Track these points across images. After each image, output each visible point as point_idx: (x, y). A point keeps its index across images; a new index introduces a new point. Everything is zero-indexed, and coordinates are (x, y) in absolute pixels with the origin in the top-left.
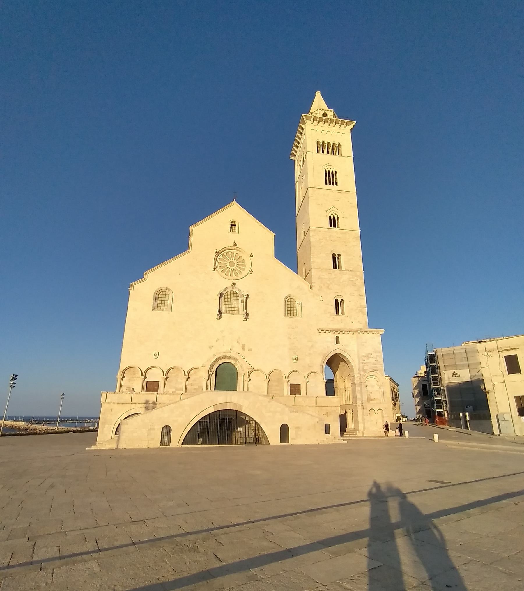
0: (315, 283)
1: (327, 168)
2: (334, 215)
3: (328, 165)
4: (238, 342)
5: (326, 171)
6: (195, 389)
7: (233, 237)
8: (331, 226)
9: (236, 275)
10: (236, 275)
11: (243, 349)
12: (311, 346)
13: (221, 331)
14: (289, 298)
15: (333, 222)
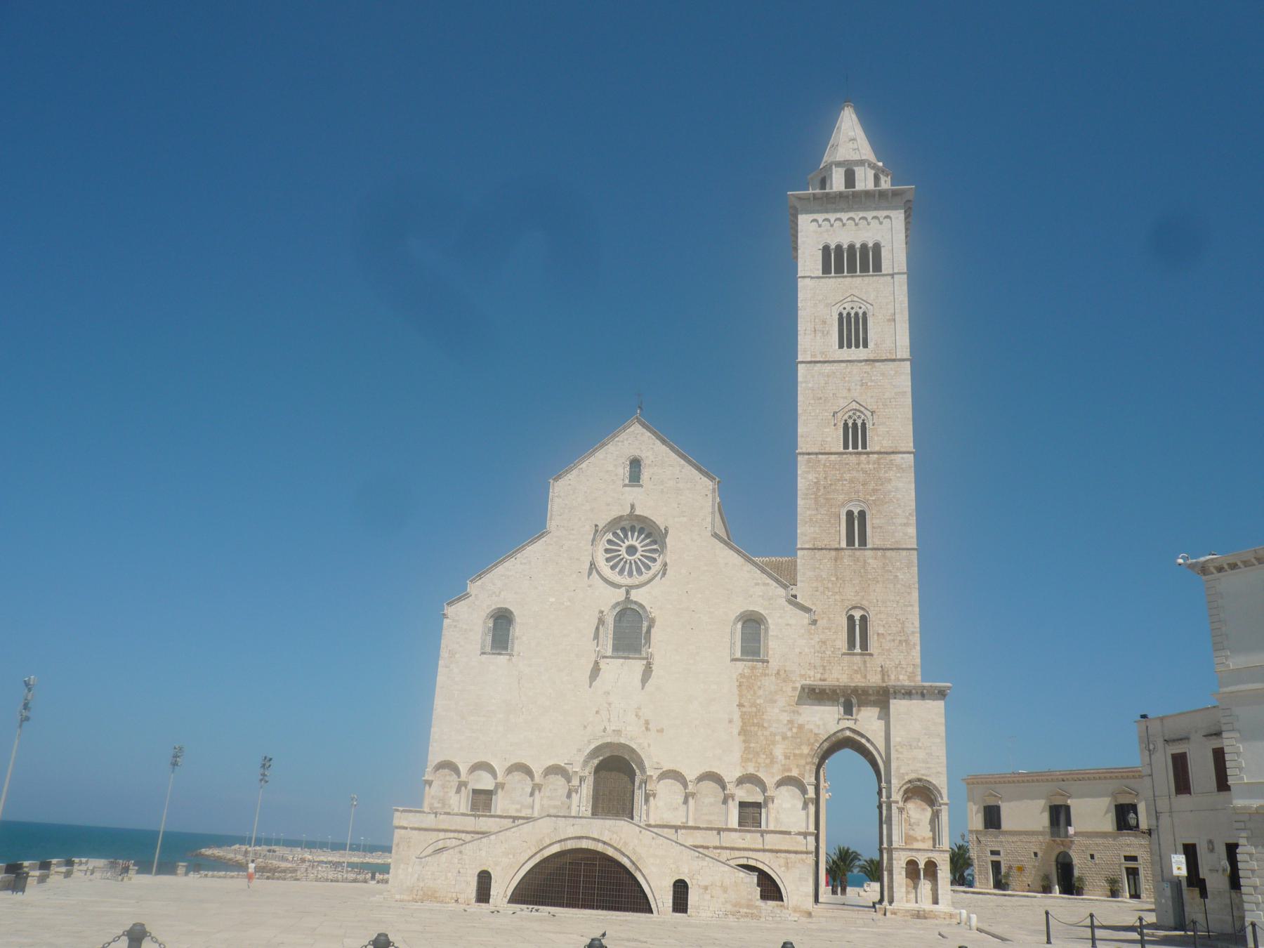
0: (802, 581)
1: (845, 309)
2: (855, 420)
3: (849, 299)
4: (636, 716)
5: (841, 314)
6: (555, 807)
7: (633, 494)
8: (846, 446)
9: (640, 572)
10: (640, 572)
11: (647, 729)
12: (788, 721)
13: (605, 693)
14: (745, 619)
15: (855, 434)
